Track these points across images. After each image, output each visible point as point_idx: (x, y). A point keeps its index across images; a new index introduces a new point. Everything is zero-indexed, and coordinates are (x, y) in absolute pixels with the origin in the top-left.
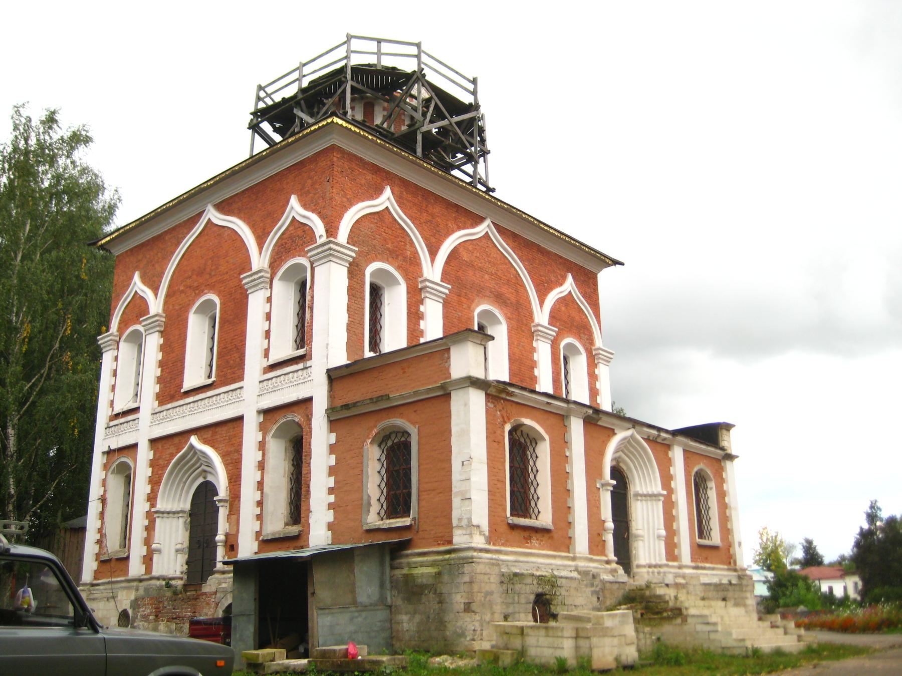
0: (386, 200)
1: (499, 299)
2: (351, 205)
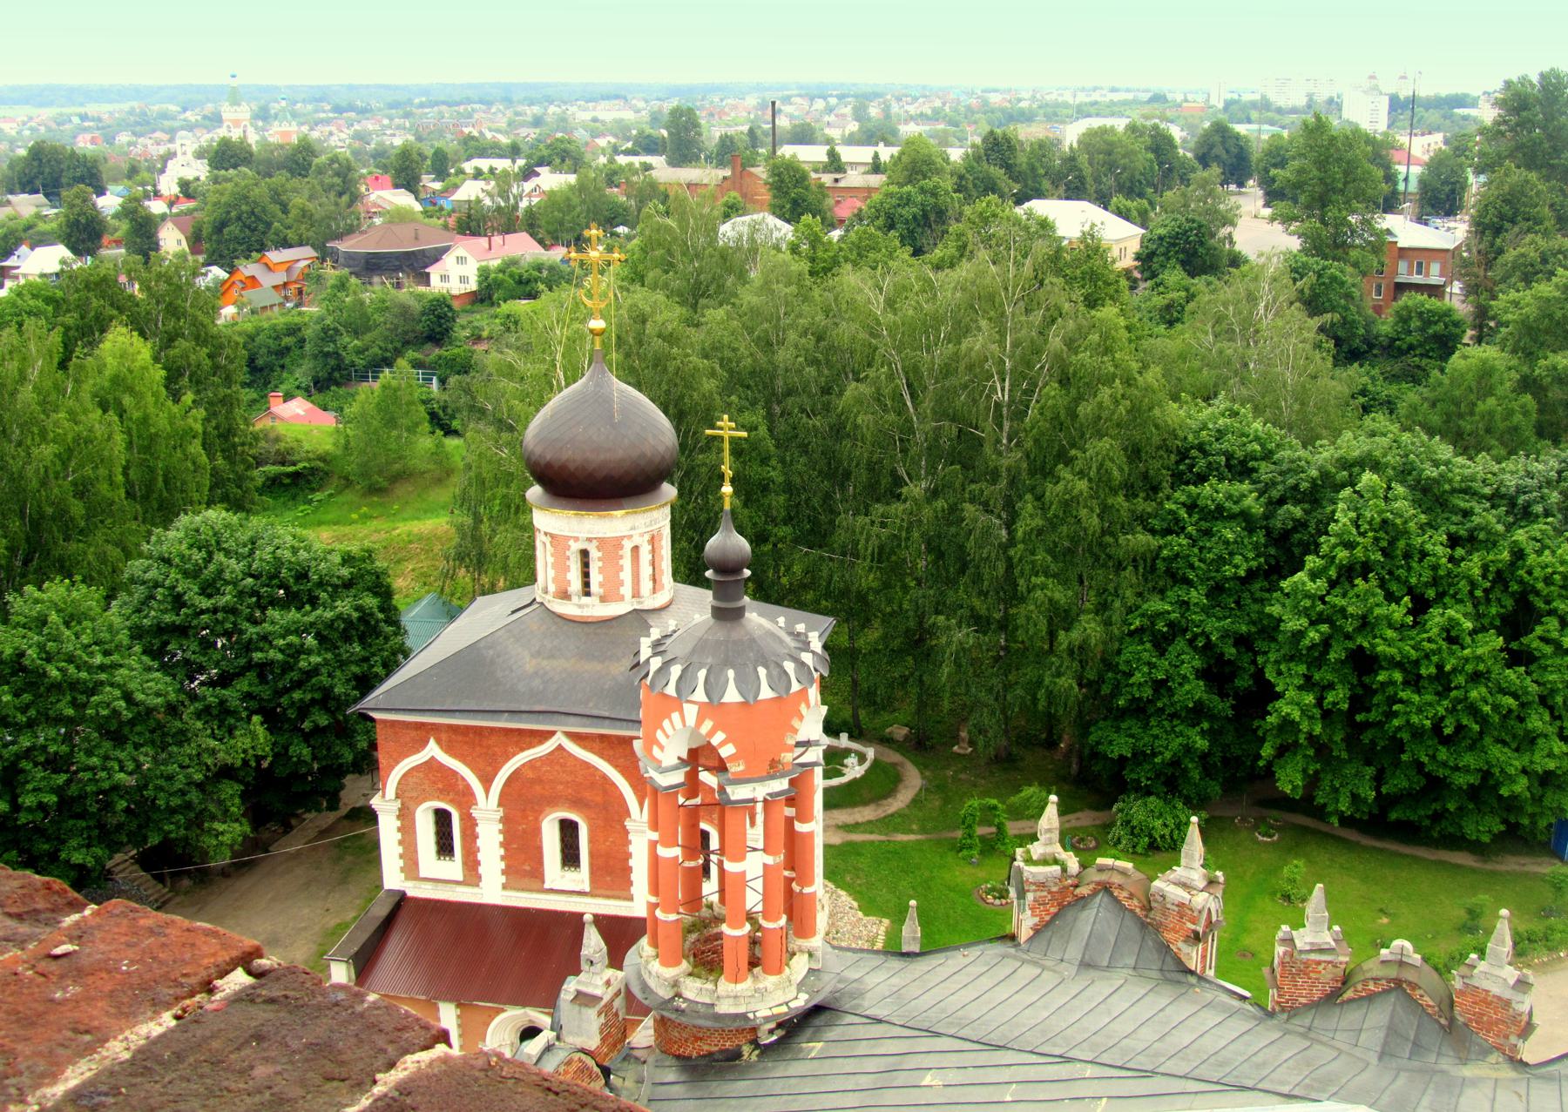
0: (433, 750)
1: (576, 803)
2: (398, 763)
